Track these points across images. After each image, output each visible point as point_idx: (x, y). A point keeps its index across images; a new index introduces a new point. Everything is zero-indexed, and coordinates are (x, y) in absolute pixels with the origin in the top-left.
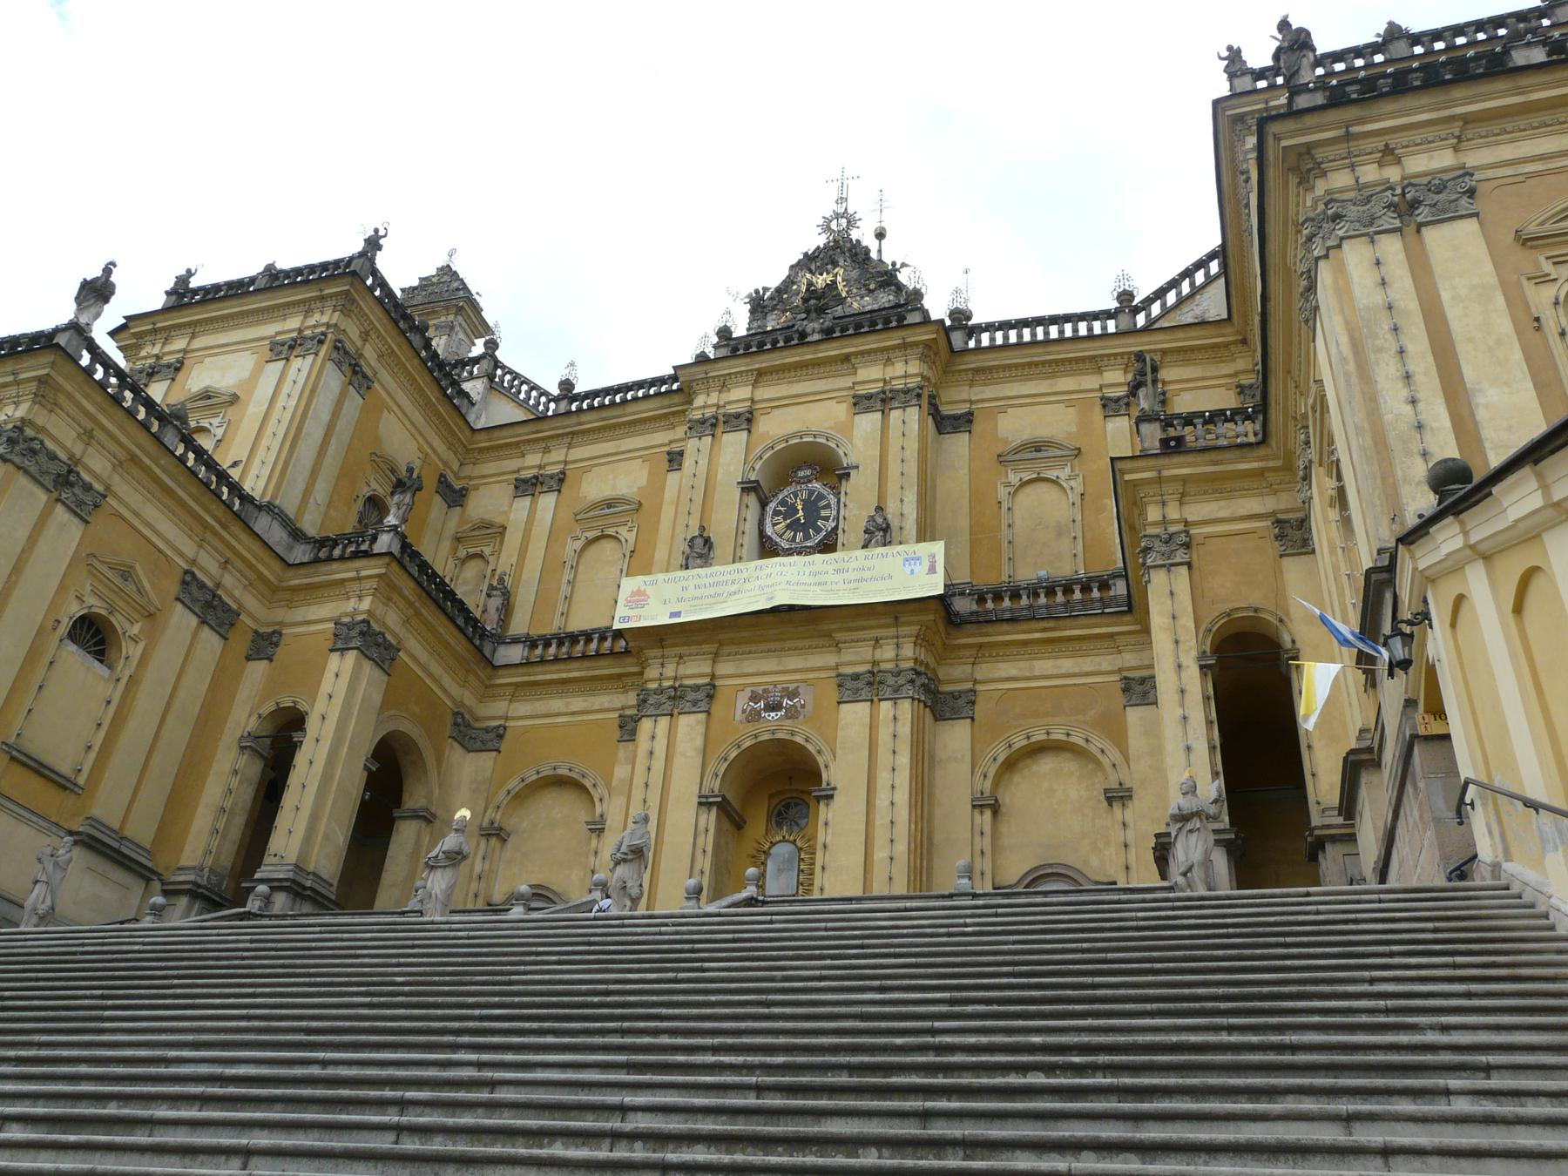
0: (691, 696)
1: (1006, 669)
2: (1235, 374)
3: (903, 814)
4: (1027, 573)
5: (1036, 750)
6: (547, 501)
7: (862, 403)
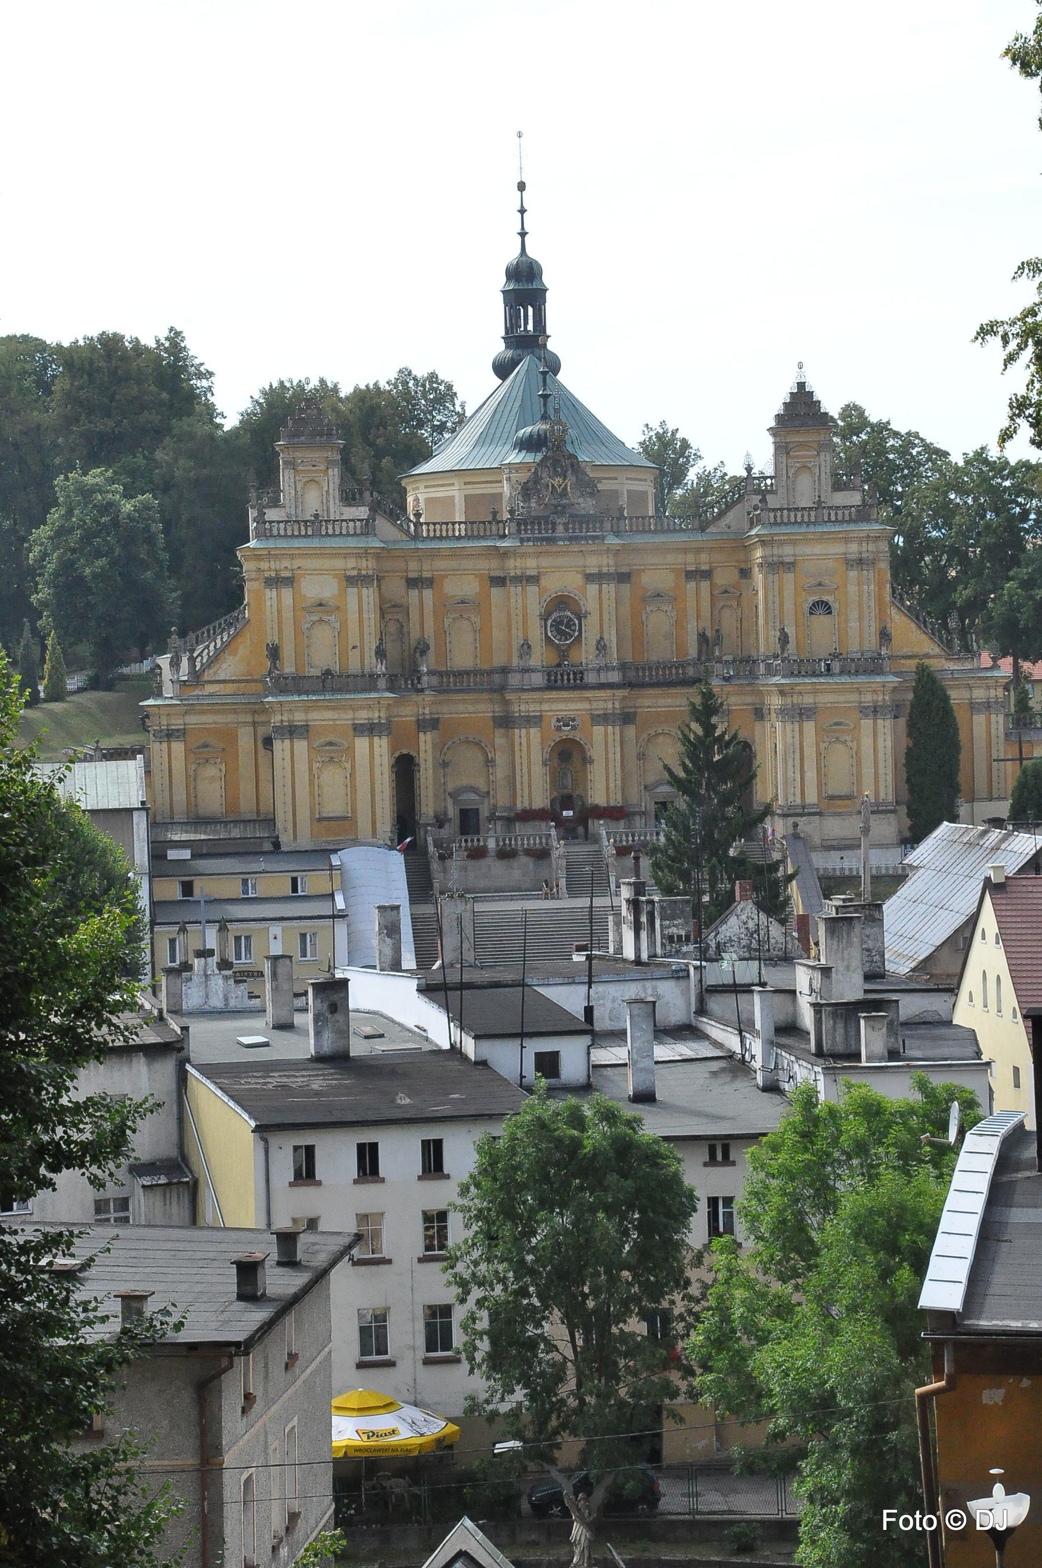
0: (533, 720)
1: (647, 702)
2: (737, 561)
3: (618, 769)
4: (654, 658)
5: (657, 735)
6: (428, 593)
7: (589, 578)
